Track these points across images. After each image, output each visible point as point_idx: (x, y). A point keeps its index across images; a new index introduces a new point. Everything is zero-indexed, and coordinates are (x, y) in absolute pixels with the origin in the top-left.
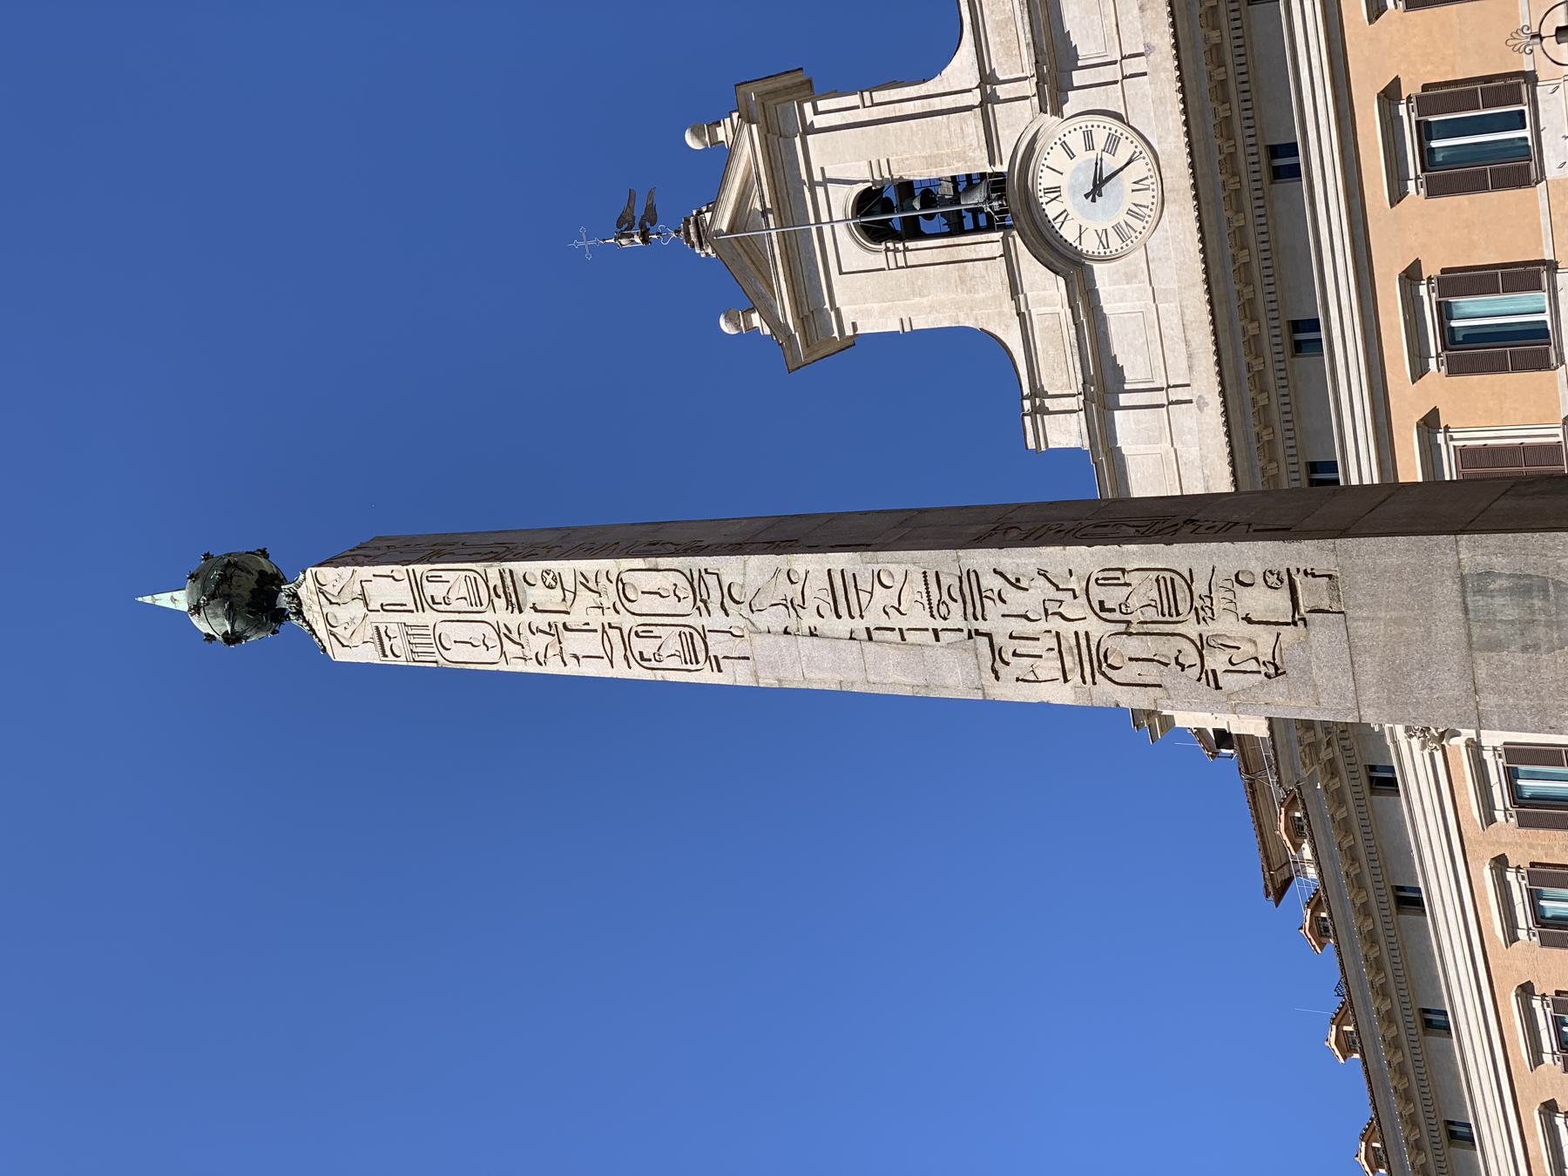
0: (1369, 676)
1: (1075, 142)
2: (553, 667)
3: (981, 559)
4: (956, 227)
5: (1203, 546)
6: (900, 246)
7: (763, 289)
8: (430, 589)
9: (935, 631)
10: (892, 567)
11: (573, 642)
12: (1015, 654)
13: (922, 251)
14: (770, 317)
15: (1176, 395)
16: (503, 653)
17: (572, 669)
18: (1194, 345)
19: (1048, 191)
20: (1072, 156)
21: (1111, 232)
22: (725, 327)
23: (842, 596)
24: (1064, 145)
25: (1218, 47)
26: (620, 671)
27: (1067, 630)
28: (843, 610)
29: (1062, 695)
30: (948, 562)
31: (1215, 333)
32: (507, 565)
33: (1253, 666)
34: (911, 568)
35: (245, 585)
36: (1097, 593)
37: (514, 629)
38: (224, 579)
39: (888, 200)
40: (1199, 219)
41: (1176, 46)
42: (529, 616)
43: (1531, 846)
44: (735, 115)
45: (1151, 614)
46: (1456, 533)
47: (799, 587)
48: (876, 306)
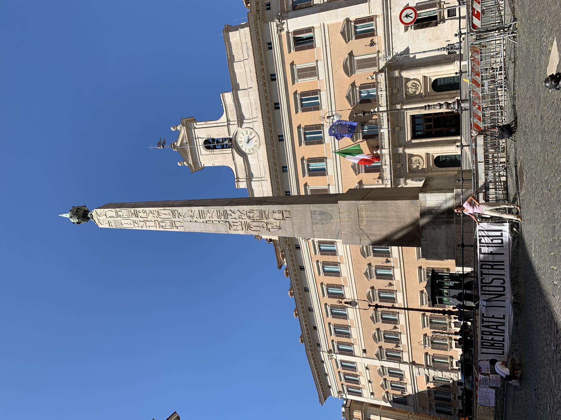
0: (295, 229)
1: (245, 133)
2: (144, 228)
3: (227, 208)
4: (223, 147)
5: (267, 206)
6: (212, 150)
7: (186, 157)
8: (119, 213)
9: (219, 221)
10: (211, 209)
11: (148, 224)
12: (233, 225)
13: (216, 151)
14: (188, 163)
15: (262, 179)
16: (134, 226)
17: (148, 229)
18: (266, 170)
19: (239, 141)
20: (244, 135)
22: (179, 164)
23: (201, 214)
24: (242, 133)
25: (269, 117)
26: (158, 229)
27: (243, 221)
28: (201, 217)
29: (242, 233)
30: (221, 209)
31: (269, 168)
32: (135, 209)
33: (276, 227)
34: (214, 209)
35: (81, 212)
36: (248, 214)
37: (136, 221)
38: (77, 211)
39: (210, 142)
40: (266, 148)
41: (262, 117)
42: (139, 218)
43: (323, 258)
44: (181, 125)
45: (258, 218)
46: (310, 204)
47: (193, 213)
48: (208, 161)
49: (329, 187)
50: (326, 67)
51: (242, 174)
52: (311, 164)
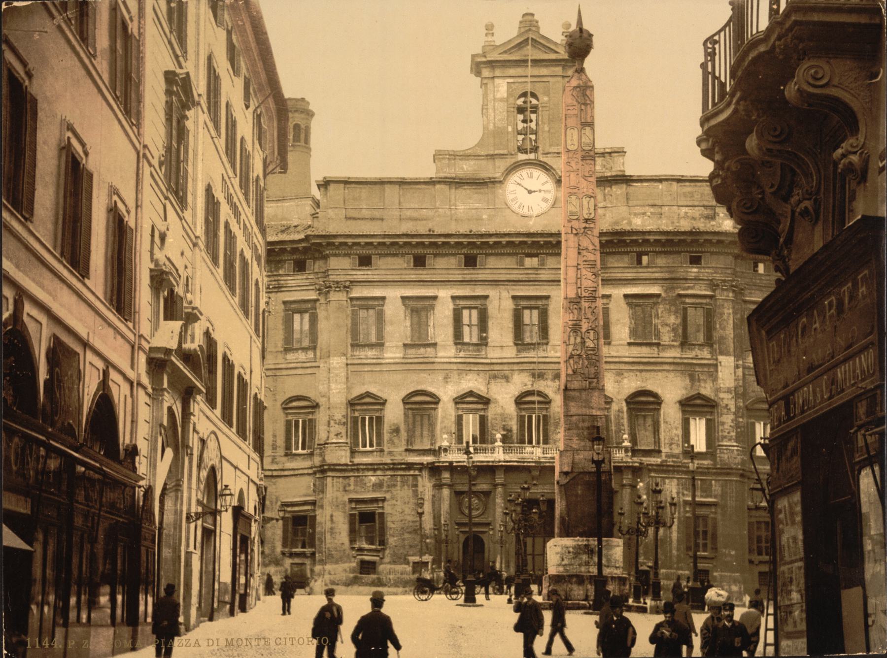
9: (580, 288)
19: (531, 174)
21: (515, 195)
24: (547, 182)
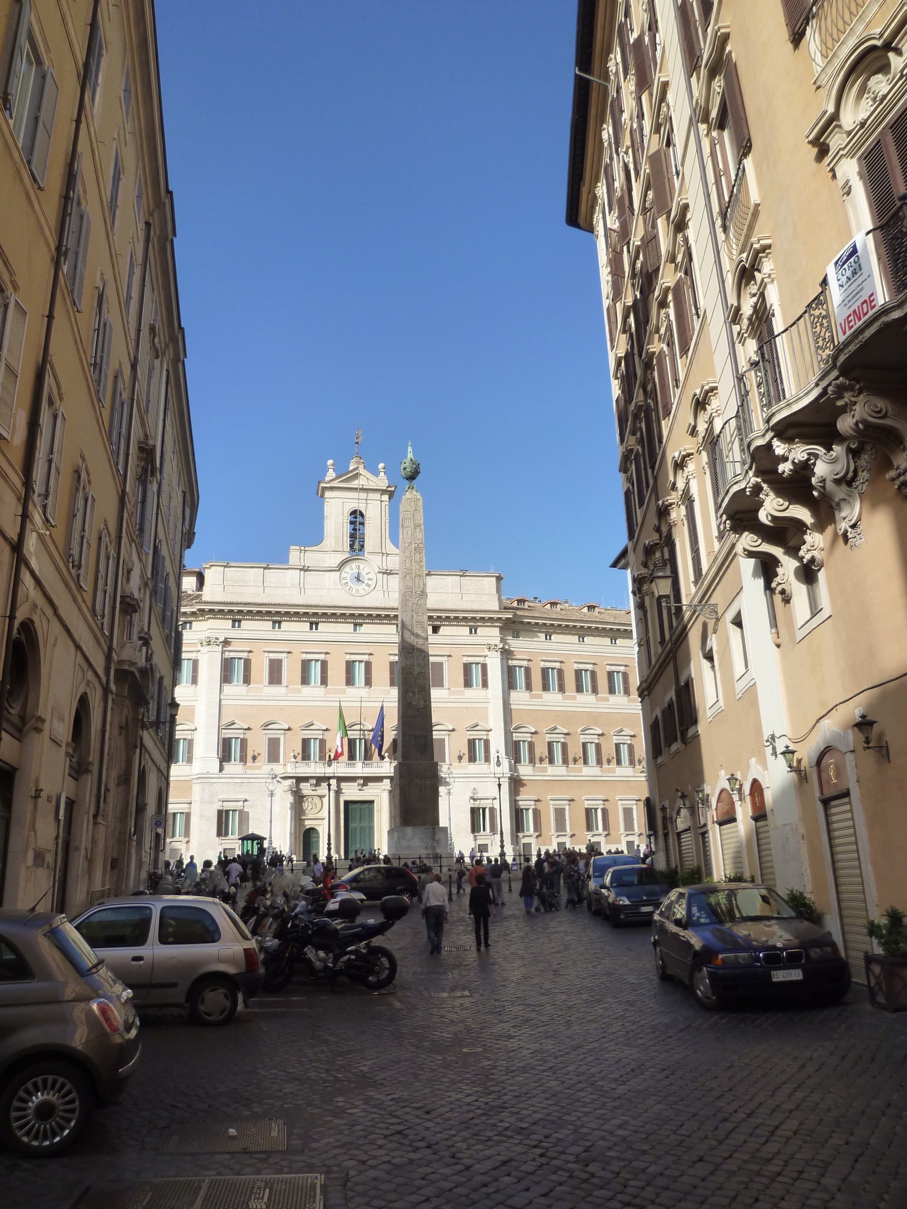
1: (370, 576)
22: (330, 462)
49: (284, 686)
50: (441, 700)
51: (312, 558)
52: (319, 664)
